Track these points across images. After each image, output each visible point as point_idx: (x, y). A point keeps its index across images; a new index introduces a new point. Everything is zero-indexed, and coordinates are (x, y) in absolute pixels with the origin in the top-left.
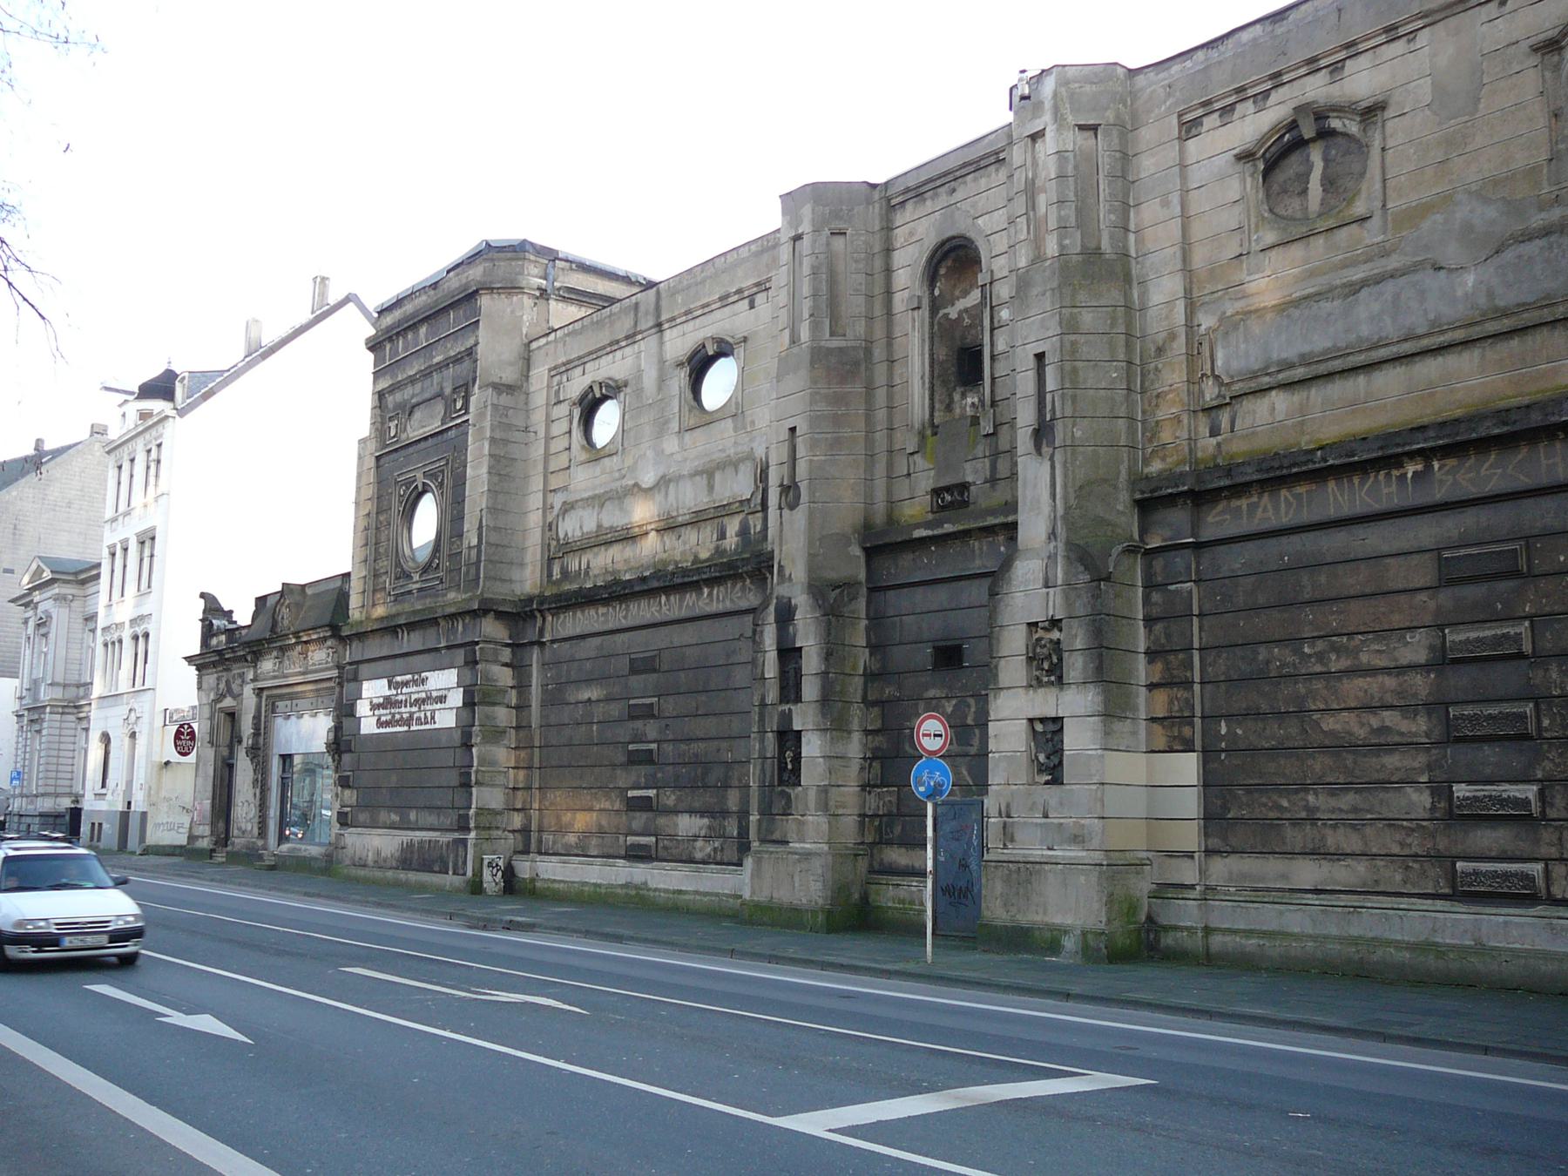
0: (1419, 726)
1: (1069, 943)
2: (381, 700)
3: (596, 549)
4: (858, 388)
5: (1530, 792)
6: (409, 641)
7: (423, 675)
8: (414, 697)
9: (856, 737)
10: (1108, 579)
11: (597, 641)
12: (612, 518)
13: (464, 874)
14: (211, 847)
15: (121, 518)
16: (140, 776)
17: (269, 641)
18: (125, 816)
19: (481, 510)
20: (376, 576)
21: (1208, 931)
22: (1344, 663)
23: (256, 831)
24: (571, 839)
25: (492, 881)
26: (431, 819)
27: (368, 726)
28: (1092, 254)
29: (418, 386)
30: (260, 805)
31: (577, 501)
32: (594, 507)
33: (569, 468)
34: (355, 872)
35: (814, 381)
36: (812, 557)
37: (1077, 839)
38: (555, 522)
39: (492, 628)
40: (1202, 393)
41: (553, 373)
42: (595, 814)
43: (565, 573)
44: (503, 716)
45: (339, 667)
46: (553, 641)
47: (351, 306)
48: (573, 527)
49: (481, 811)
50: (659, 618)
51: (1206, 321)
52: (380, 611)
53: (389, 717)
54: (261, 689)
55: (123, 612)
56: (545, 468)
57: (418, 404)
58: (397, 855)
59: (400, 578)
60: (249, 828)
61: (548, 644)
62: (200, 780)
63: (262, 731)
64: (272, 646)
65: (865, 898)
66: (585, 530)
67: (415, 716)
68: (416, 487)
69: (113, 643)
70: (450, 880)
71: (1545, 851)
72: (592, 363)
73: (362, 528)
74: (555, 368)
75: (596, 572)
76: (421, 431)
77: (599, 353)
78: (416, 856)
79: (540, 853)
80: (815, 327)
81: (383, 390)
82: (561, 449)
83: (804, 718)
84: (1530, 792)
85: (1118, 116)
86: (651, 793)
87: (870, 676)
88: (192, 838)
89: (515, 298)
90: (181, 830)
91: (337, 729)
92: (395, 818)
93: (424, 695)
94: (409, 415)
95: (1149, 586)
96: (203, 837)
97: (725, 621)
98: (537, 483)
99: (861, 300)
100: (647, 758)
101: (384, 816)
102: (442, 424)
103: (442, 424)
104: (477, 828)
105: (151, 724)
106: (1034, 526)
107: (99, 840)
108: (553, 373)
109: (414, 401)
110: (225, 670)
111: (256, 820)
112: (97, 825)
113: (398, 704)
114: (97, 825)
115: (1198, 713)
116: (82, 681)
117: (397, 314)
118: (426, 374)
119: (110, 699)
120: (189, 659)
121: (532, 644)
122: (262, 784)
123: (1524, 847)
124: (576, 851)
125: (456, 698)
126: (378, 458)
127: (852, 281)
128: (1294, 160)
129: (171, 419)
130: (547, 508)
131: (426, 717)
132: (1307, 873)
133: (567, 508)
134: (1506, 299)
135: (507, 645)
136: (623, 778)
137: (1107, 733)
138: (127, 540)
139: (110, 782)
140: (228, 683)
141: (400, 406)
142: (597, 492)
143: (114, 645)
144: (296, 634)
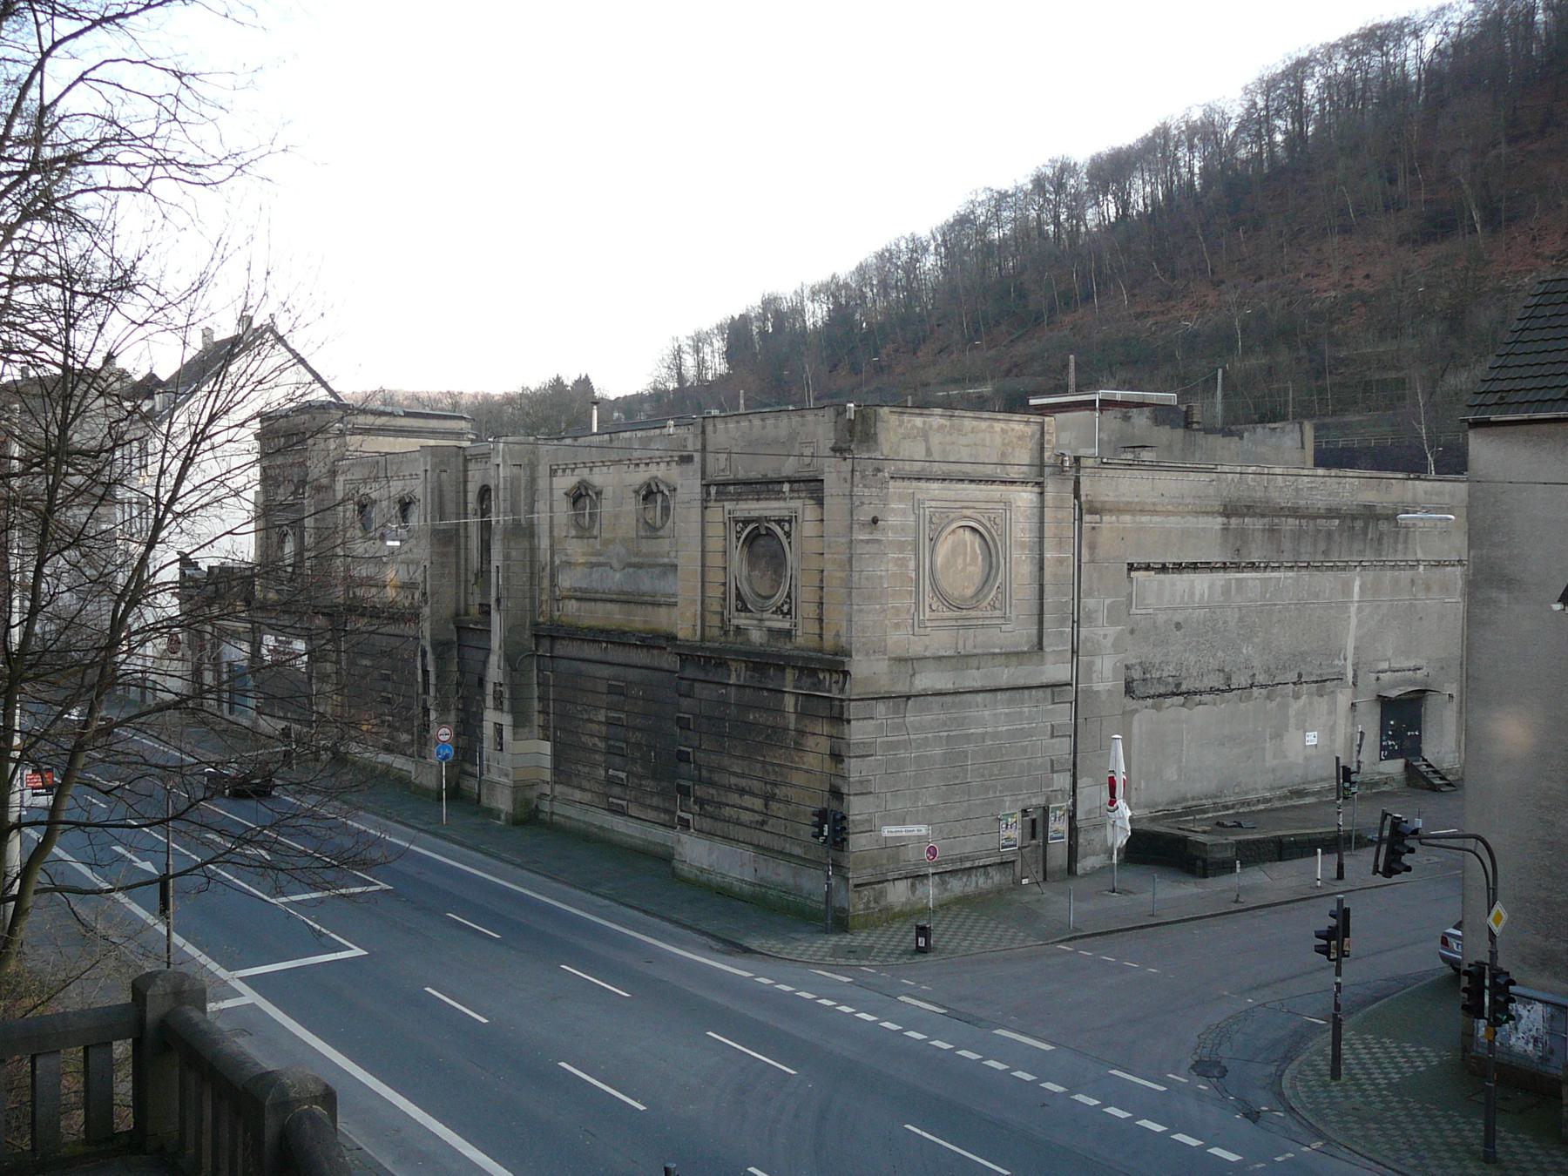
0: (602, 745)
1: (503, 816)
4: (452, 549)
5: (623, 775)
9: (453, 713)
10: (516, 670)
21: (552, 813)
22: (585, 717)
28: (517, 524)
37: (507, 775)
39: (320, 621)
40: (555, 592)
51: (557, 562)
65: (458, 784)
71: (628, 797)
80: (433, 519)
83: (431, 701)
84: (623, 775)
85: (529, 460)
87: (459, 684)
95: (539, 670)
99: (454, 505)
106: (495, 642)
115: (552, 725)
123: (623, 795)
127: (450, 495)
128: (582, 500)
132: (578, 795)
134: (627, 588)
137: (514, 734)
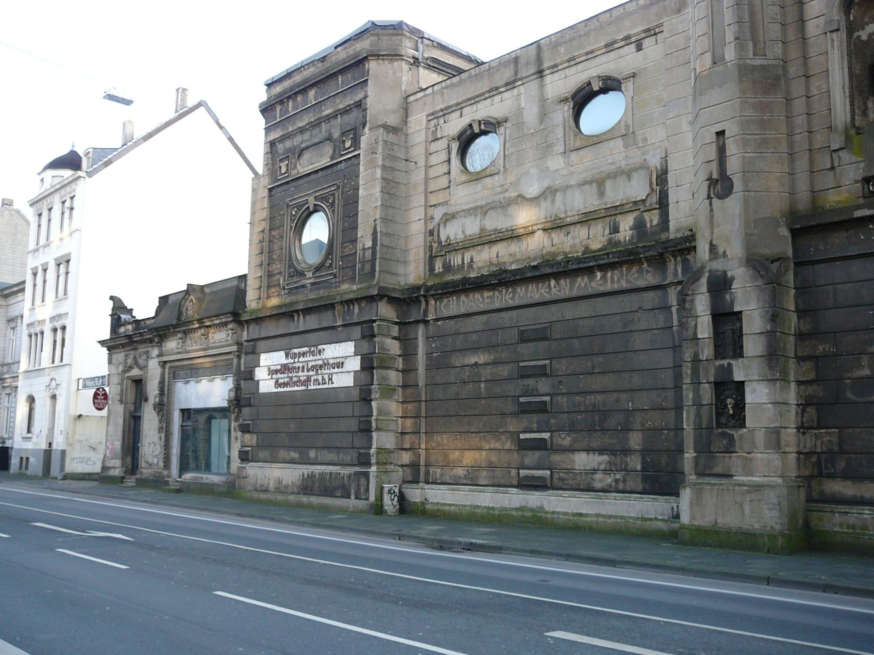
2: (279, 367)
3: (479, 247)
6: (304, 322)
7: (320, 347)
8: (310, 364)
9: (793, 386)
11: (484, 318)
12: (495, 222)
13: (367, 499)
14: (122, 475)
15: (41, 250)
16: (61, 423)
17: (175, 326)
18: (48, 453)
19: (375, 221)
20: (270, 275)
23: (161, 464)
24: (460, 472)
25: (390, 503)
26: (332, 456)
29: (307, 135)
30: (165, 445)
31: (458, 212)
32: (476, 216)
33: (449, 187)
34: (256, 495)
35: (743, 92)
36: (748, 236)
38: (436, 230)
39: (385, 310)
41: (430, 118)
42: (484, 453)
43: (447, 268)
44: (394, 378)
45: (239, 344)
46: (437, 320)
47: (202, 109)
48: (452, 232)
49: (380, 450)
50: (548, 297)
52: (274, 301)
53: (286, 380)
54: (165, 362)
55: (45, 312)
56: (426, 189)
57: (307, 148)
58: (298, 483)
59: (293, 276)
60: (155, 461)
61: (431, 322)
62: (111, 428)
63: (166, 392)
64: (176, 330)
65: (807, 524)
66: (468, 233)
67: (312, 379)
68: (308, 207)
69: (36, 335)
70: (352, 503)
72: (469, 108)
73: (258, 241)
74: (433, 114)
75: (479, 265)
76: (311, 167)
77: (477, 99)
78: (317, 484)
79: (427, 482)
81: (274, 140)
82: (440, 174)
86: (546, 435)
88: (104, 468)
89: (396, 64)
90: (88, 462)
91: (237, 388)
92: (295, 455)
93: (321, 362)
94: (299, 157)
96: (114, 468)
97: (620, 298)
98: (418, 200)
99: (777, 27)
100: (542, 408)
101: (283, 454)
102: (331, 160)
103: (331, 160)
104: (377, 463)
105: (69, 388)
107: (27, 468)
108: (430, 118)
109: (303, 145)
110: (133, 349)
111: (162, 456)
112: (24, 459)
114: (24, 459)
116: (6, 362)
117: (287, 84)
118: (315, 125)
120: (102, 343)
121: (417, 322)
122: (165, 429)
124: (465, 481)
125: (355, 364)
126: (270, 190)
129: (82, 179)
130: (429, 219)
131: (323, 379)
133: (448, 218)
135: (396, 323)
136: (513, 425)
138: (47, 263)
139: (36, 429)
140: (135, 358)
141: (292, 150)
142: (479, 204)
143: (36, 336)
144: (200, 321)
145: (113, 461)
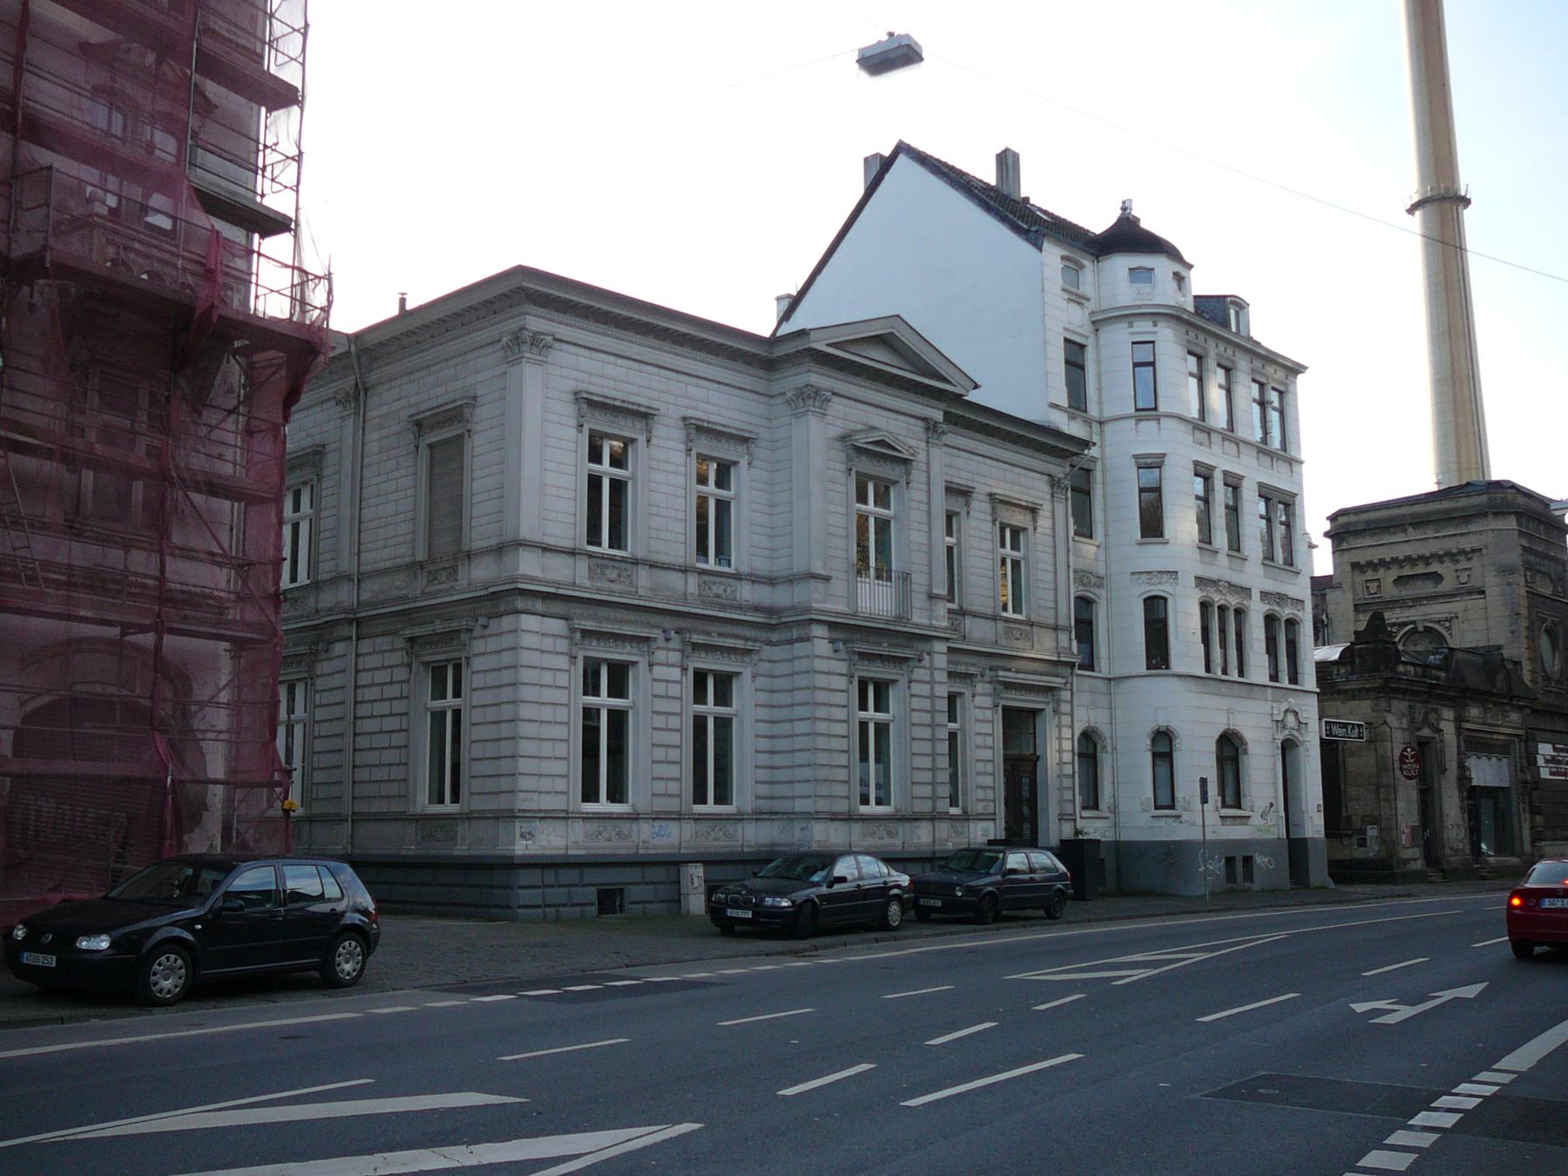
27: (1545, 773)
60: (1461, 847)
96: (1415, 860)
107: (1249, 876)
113: (1559, 762)
119: (1237, 686)
140: (1426, 714)
145: (1410, 850)
